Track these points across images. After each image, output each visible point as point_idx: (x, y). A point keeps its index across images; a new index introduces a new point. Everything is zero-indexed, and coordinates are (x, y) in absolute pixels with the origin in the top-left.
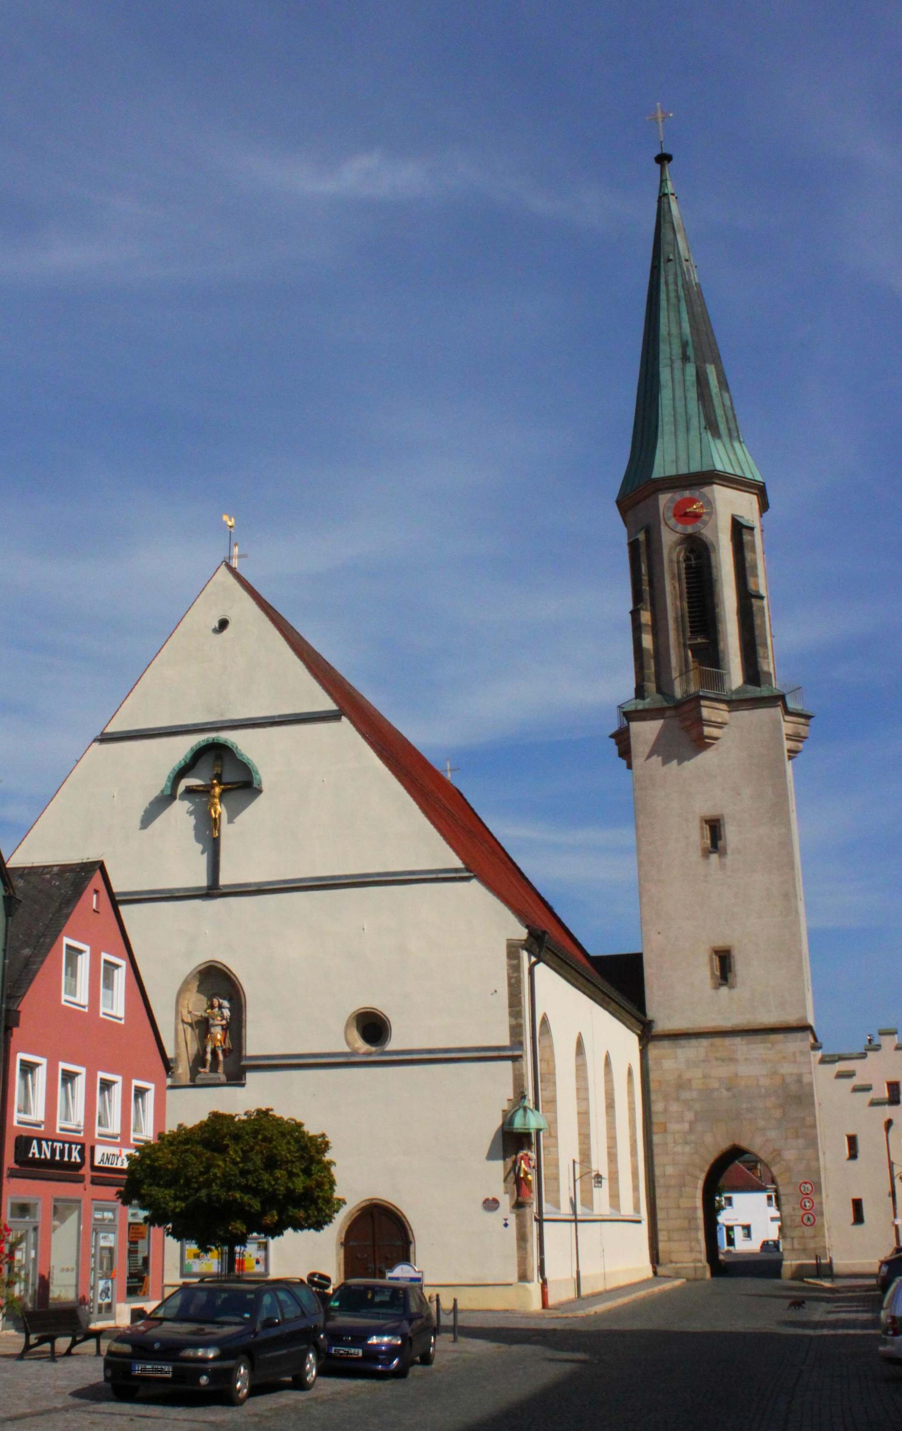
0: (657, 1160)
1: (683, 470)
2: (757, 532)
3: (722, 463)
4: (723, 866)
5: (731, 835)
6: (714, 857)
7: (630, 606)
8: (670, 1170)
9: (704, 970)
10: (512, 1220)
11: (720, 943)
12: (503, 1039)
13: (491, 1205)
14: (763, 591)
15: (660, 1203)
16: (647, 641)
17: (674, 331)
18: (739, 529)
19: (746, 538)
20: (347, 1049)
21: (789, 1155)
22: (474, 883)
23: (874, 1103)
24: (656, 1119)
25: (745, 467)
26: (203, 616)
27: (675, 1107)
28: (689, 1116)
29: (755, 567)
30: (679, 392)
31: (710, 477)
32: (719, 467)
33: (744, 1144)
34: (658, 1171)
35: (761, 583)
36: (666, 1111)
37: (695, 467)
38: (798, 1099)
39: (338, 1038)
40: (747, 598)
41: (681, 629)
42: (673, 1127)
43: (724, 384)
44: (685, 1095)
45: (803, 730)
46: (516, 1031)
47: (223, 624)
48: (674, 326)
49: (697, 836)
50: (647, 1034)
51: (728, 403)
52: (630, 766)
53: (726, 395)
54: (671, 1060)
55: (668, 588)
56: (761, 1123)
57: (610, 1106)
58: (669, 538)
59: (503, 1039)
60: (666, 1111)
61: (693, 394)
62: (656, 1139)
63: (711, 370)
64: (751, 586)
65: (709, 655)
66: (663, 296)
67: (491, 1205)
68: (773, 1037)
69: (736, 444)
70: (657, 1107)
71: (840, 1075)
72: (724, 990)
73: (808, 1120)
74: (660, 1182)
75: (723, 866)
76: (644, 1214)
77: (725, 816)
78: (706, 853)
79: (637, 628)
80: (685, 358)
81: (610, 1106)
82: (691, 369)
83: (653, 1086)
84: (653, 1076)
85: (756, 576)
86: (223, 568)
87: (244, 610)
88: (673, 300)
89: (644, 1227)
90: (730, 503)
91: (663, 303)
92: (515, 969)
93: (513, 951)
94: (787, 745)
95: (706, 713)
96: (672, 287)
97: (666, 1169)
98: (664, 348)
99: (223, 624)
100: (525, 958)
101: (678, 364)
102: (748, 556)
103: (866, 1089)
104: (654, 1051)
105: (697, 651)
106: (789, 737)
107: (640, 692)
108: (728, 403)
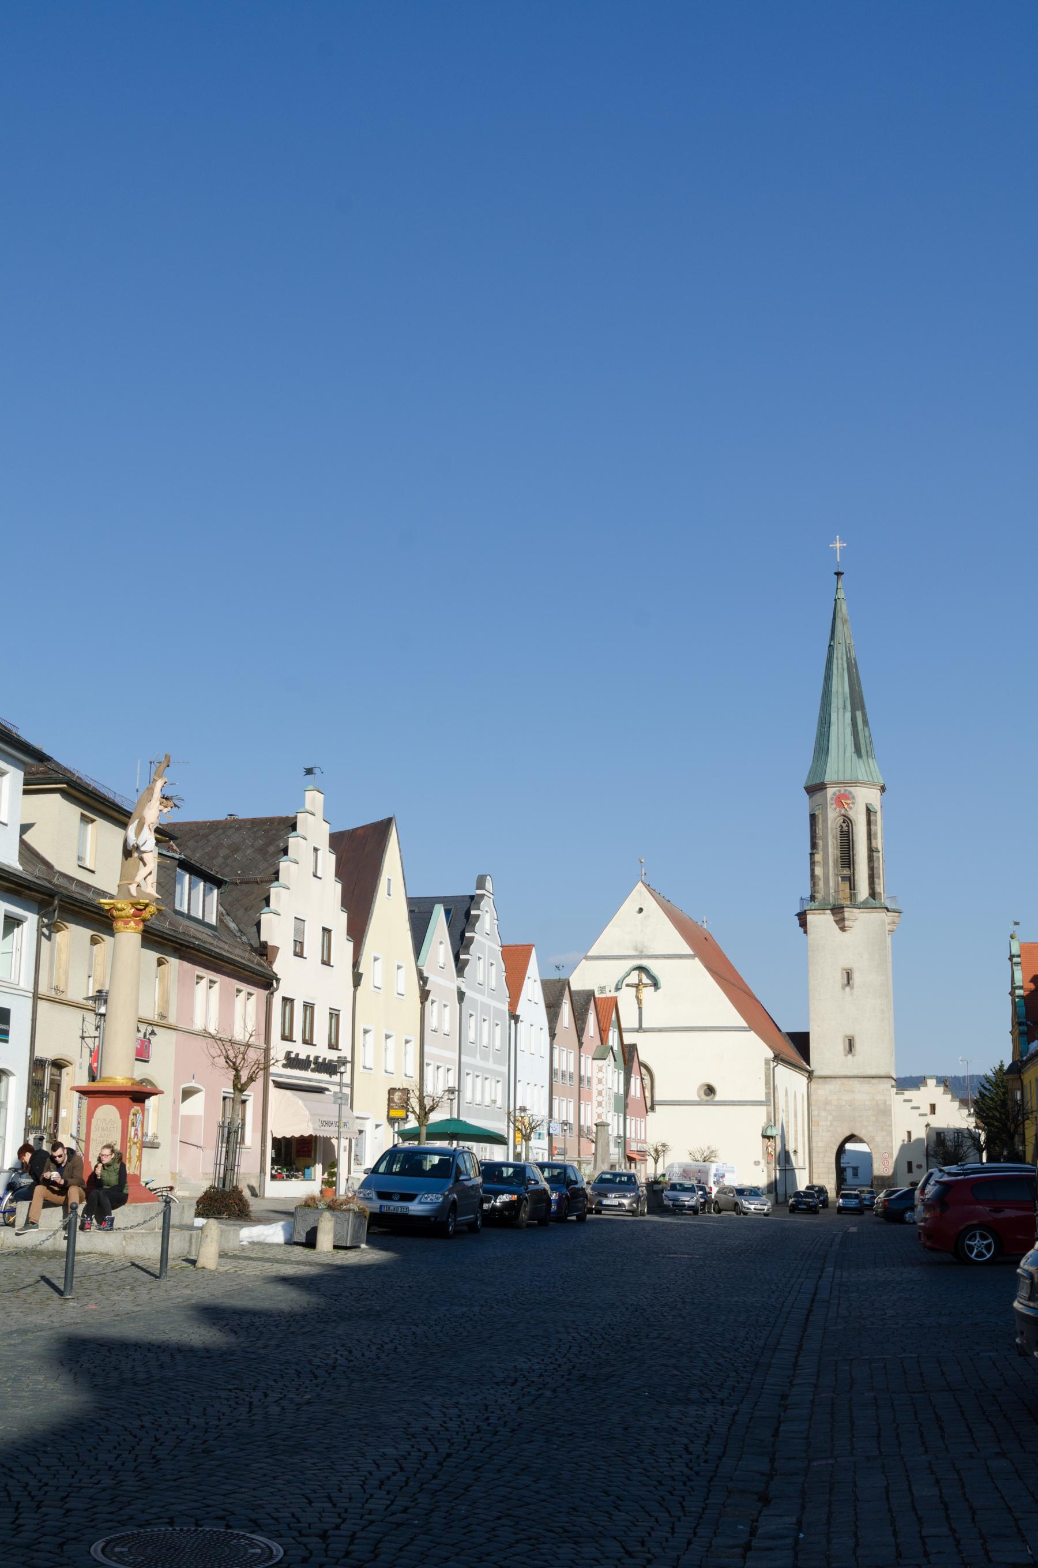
0: (814, 1139)
1: (841, 778)
2: (879, 814)
3: (862, 776)
4: (852, 994)
5: (856, 977)
6: (848, 989)
7: (809, 851)
8: (820, 1144)
9: (841, 1046)
10: (765, 1169)
11: (849, 1033)
12: (764, 1099)
13: (757, 1163)
14: (880, 849)
15: (814, 1160)
16: (818, 871)
17: (840, 690)
18: (869, 811)
19: (872, 818)
20: (697, 1099)
21: (878, 1139)
22: (752, 1034)
23: (921, 1115)
24: (814, 1119)
25: (874, 775)
26: (629, 906)
27: (823, 1114)
28: (830, 1118)
29: (876, 834)
30: (841, 730)
31: (856, 783)
32: (860, 778)
33: (856, 1133)
34: (814, 1144)
35: (879, 843)
36: (818, 1115)
37: (848, 777)
38: (884, 1112)
39: (693, 1094)
40: (871, 851)
41: (835, 865)
42: (822, 1123)
43: (865, 722)
44: (829, 1108)
45: (897, 920)
46: (767, 1094)
47: (641, 910)
48: (841, 686)
49: (840, 978)
50: (810, 1075)
51: (867, 734)
52: (805, 932)
53: (866, 729)
54: (821, 1090)
55: (830, 843)
56: (865, 1123)
57: (796, 1116)
58: (832, 817)
59: (764, 1099)
60: (818, 1115)
61: (849, 730)
62: (814, 1129)
63: (859, 714)
64: (874, 845)
65: (851, 881)
66: (835, 667)
67: (757, 1163)
68: (872, 1080)
69: (870, 761)
70: (815, 1113)
71: (905, 1101)
72: (850, 1056)
73: (888, 1123)
74: (815, 1150)
75: (852, 994)
76: (807, 1166)
77: (855, 970)
78: (843, 988)
79: (813, 863)
80: (844, 708)
81: (796, 1116)
82: (848, 715)
83: (813, 1102)
84: (813, 1098)
85: (876, 839)
86: (640, 883)
87: (651, 905)
88: (840, 670)
89: (807, 1171)
90: (866, 796)
91: (835, 671)
92: (768, 1069)
93: (767, 1062)
94: (888, 928)
95: (846, 915)
96: (840, 661)
97: (819, 1143)
98: (834, 700)
99: (641, 910)
100: (772, 1064)
101: (841, 710)
102: (873, 827)
103: (918, 1108)
104: (813, 1085)
105: (844, 878)
106: (889, 924)
107: (813, 898)
108: (867, 734)
